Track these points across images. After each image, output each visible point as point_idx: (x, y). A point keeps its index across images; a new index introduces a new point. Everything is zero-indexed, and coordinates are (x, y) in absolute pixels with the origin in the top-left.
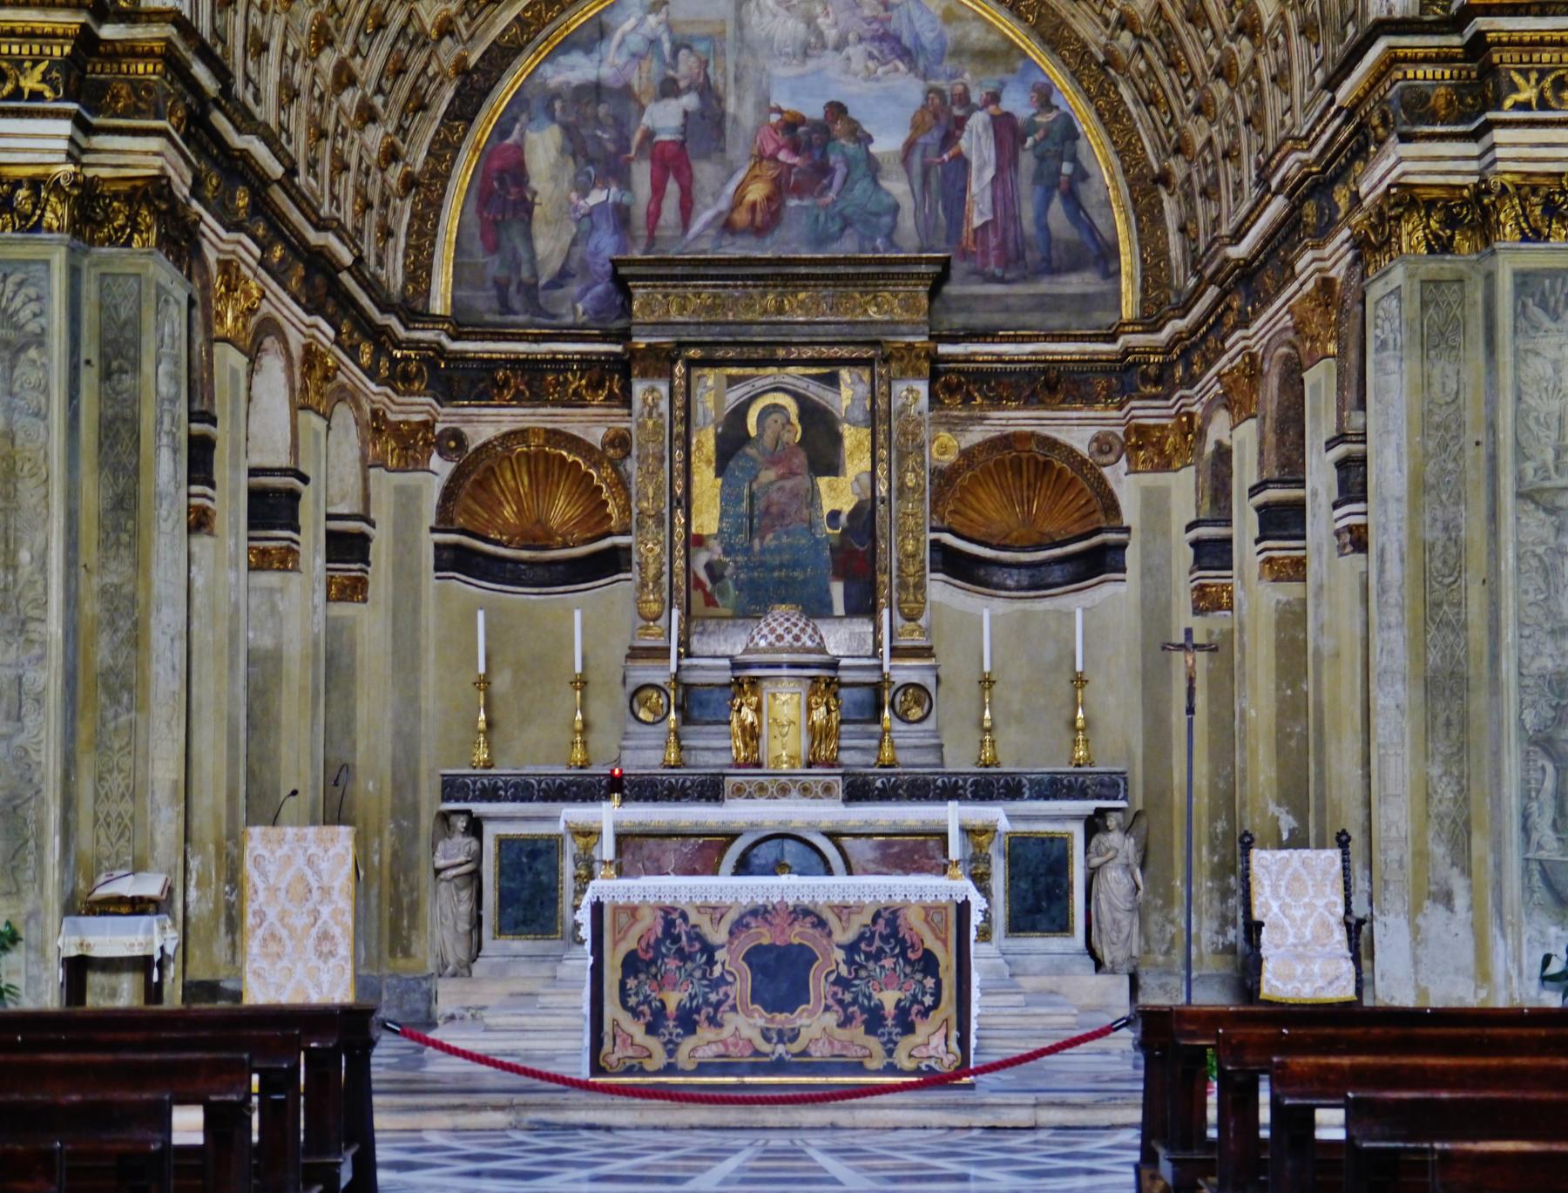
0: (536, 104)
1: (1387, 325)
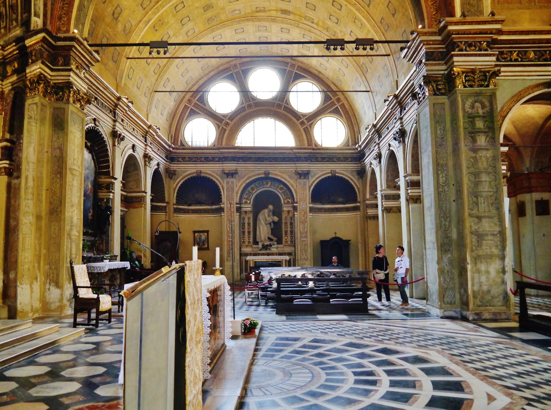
1: (32, 112)
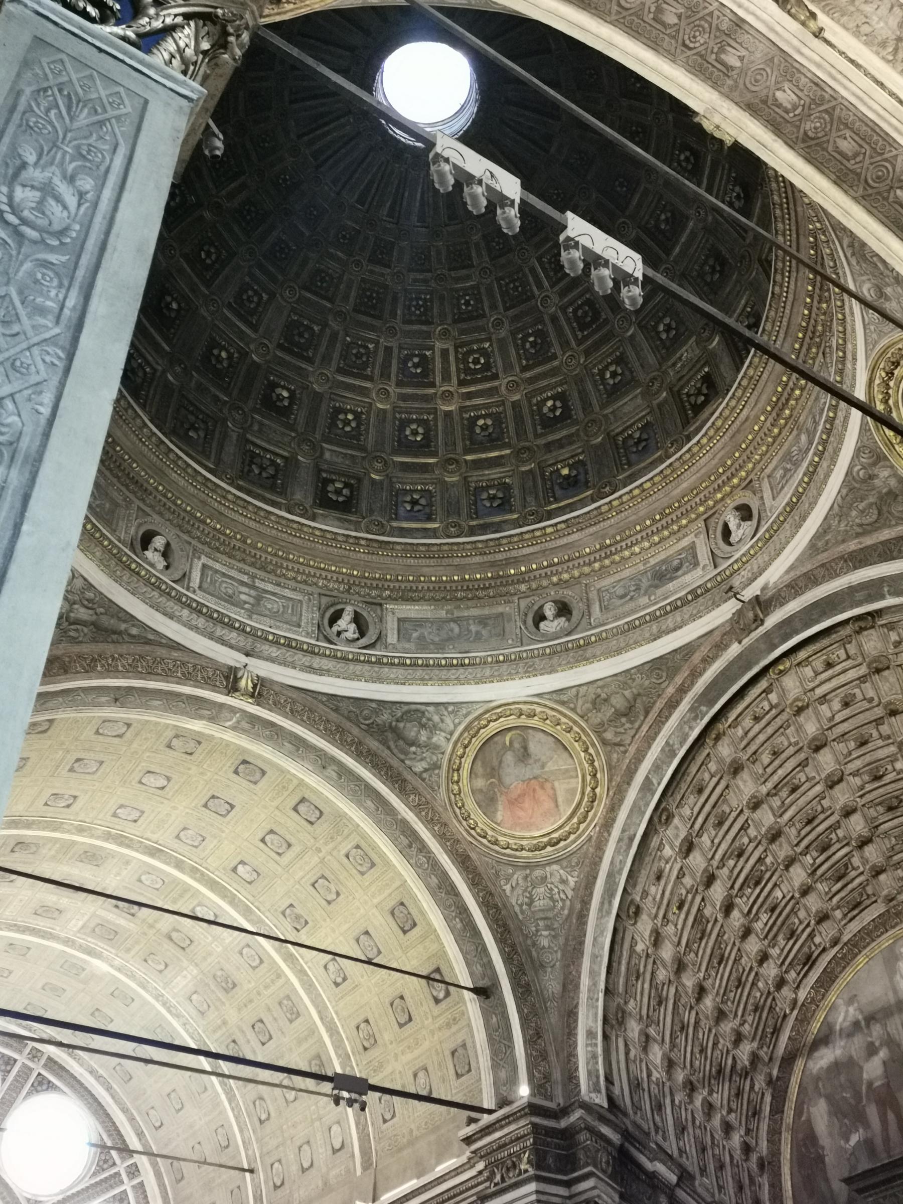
0: (811, 1088)
